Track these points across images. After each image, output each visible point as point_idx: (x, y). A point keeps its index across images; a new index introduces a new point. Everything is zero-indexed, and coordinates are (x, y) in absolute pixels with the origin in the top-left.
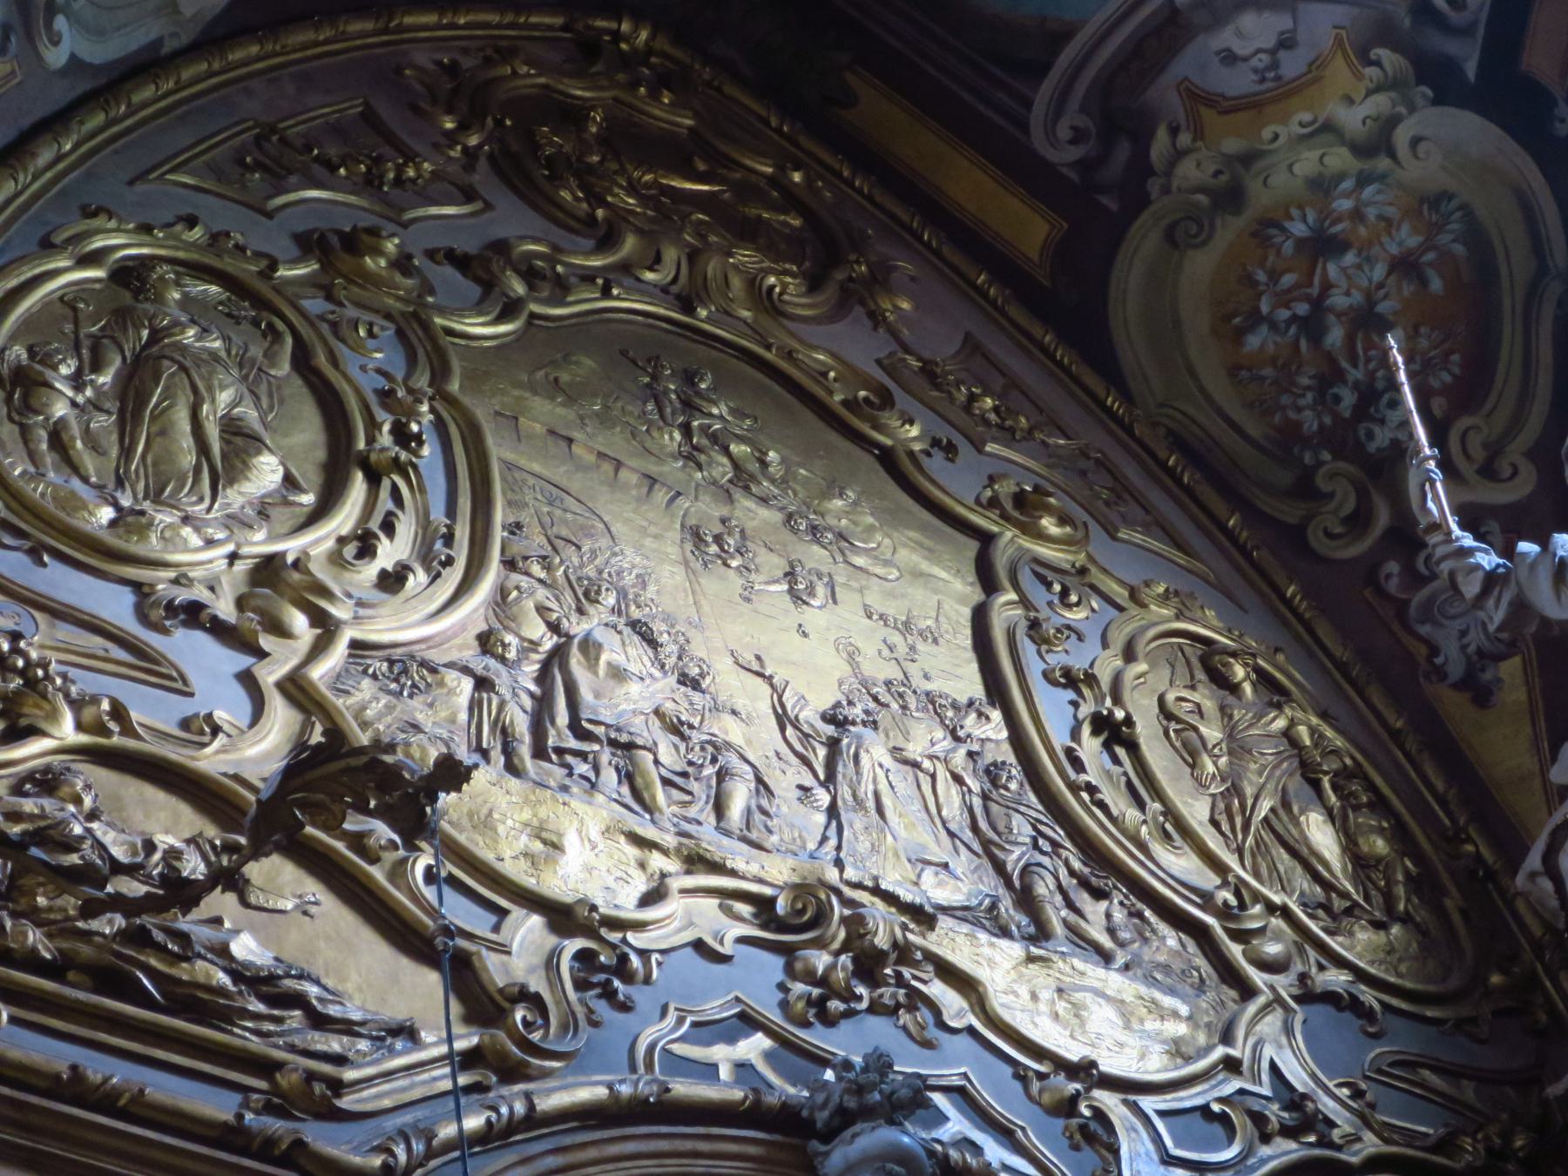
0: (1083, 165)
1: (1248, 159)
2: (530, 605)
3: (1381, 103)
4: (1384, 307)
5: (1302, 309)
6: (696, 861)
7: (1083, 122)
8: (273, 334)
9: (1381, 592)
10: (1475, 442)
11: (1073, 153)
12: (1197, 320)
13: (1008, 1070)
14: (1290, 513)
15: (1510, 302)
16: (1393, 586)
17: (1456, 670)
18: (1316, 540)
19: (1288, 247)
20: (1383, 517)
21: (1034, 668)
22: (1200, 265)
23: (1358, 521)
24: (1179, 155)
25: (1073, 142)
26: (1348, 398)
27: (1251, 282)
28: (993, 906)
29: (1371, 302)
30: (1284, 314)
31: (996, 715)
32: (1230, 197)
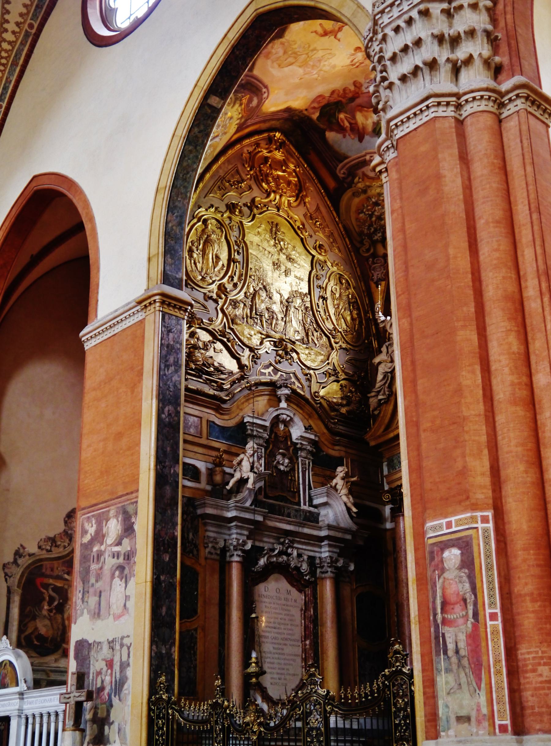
0: (343, 178)
1: (369, 187)
2: (251, 285)
5: (370, 213)
6: (268, 336)
7: (345, 171)
8: (222, 231)
11: (342, 176)
12: (353, 209)
13: (300, 368)
14: (358, 245)
16: (370, 263)
17: (375, 280)
18: (361, 251)
20: (372, 251)
21: (316, 284)
22: (356, 200)
23: (368, 250)
24: (359, 182)
25: (343, 174)
26: (372, 230)
27: (363, 206)
28: (303, 339)
30: (367, 213)
31: (309, 297)
32: (365, 191)
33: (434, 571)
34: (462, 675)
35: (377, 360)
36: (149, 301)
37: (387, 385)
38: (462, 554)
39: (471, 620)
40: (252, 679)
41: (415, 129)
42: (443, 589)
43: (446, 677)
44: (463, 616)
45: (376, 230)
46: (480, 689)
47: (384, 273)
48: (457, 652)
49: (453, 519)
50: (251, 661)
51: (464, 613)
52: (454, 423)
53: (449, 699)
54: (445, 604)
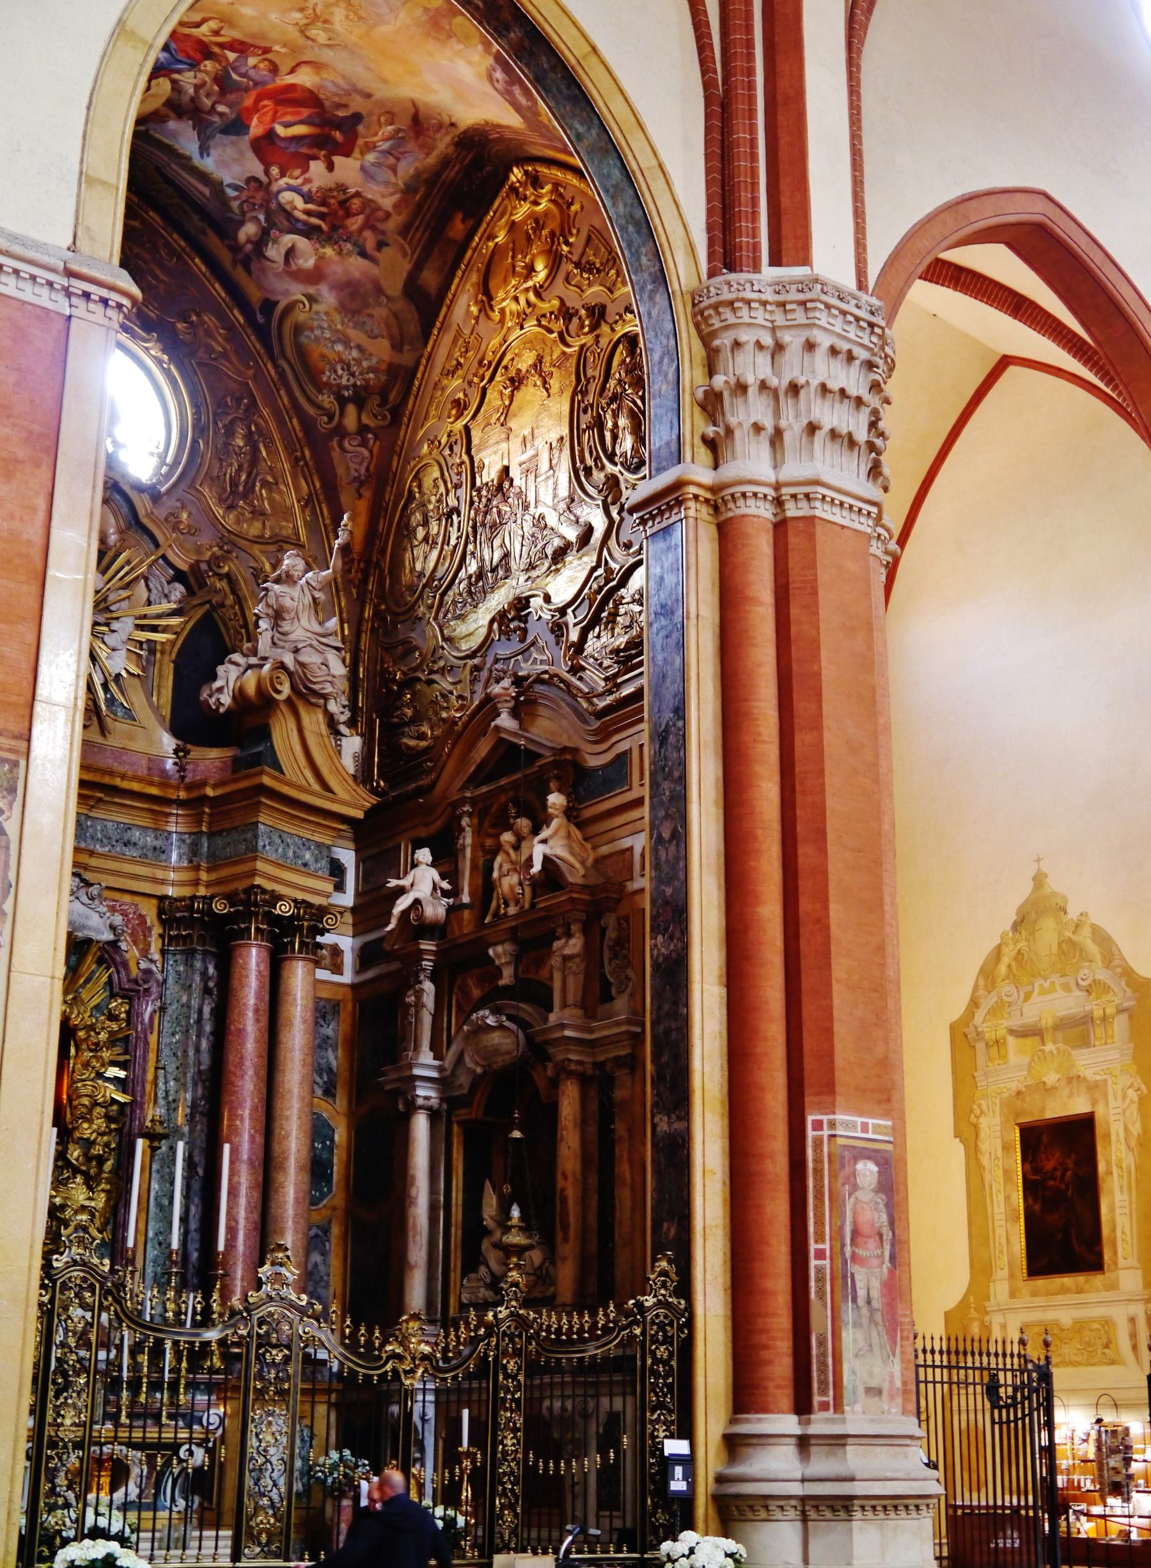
33: (844, 1184)
34: (874, 1333)
36: (105, 293)
38: (879, 1172)
39: (887, 1264)
41: (843, 527)
42: (855, 1214)
43: (854, 1333)
44: (878, 1257)
46: (894, 1355)
48: (869, 1302)
49: (871, 1121)
51: (879, 1252)
52: (876, 991)
53: (857, 1363)
54: (855, 1233)
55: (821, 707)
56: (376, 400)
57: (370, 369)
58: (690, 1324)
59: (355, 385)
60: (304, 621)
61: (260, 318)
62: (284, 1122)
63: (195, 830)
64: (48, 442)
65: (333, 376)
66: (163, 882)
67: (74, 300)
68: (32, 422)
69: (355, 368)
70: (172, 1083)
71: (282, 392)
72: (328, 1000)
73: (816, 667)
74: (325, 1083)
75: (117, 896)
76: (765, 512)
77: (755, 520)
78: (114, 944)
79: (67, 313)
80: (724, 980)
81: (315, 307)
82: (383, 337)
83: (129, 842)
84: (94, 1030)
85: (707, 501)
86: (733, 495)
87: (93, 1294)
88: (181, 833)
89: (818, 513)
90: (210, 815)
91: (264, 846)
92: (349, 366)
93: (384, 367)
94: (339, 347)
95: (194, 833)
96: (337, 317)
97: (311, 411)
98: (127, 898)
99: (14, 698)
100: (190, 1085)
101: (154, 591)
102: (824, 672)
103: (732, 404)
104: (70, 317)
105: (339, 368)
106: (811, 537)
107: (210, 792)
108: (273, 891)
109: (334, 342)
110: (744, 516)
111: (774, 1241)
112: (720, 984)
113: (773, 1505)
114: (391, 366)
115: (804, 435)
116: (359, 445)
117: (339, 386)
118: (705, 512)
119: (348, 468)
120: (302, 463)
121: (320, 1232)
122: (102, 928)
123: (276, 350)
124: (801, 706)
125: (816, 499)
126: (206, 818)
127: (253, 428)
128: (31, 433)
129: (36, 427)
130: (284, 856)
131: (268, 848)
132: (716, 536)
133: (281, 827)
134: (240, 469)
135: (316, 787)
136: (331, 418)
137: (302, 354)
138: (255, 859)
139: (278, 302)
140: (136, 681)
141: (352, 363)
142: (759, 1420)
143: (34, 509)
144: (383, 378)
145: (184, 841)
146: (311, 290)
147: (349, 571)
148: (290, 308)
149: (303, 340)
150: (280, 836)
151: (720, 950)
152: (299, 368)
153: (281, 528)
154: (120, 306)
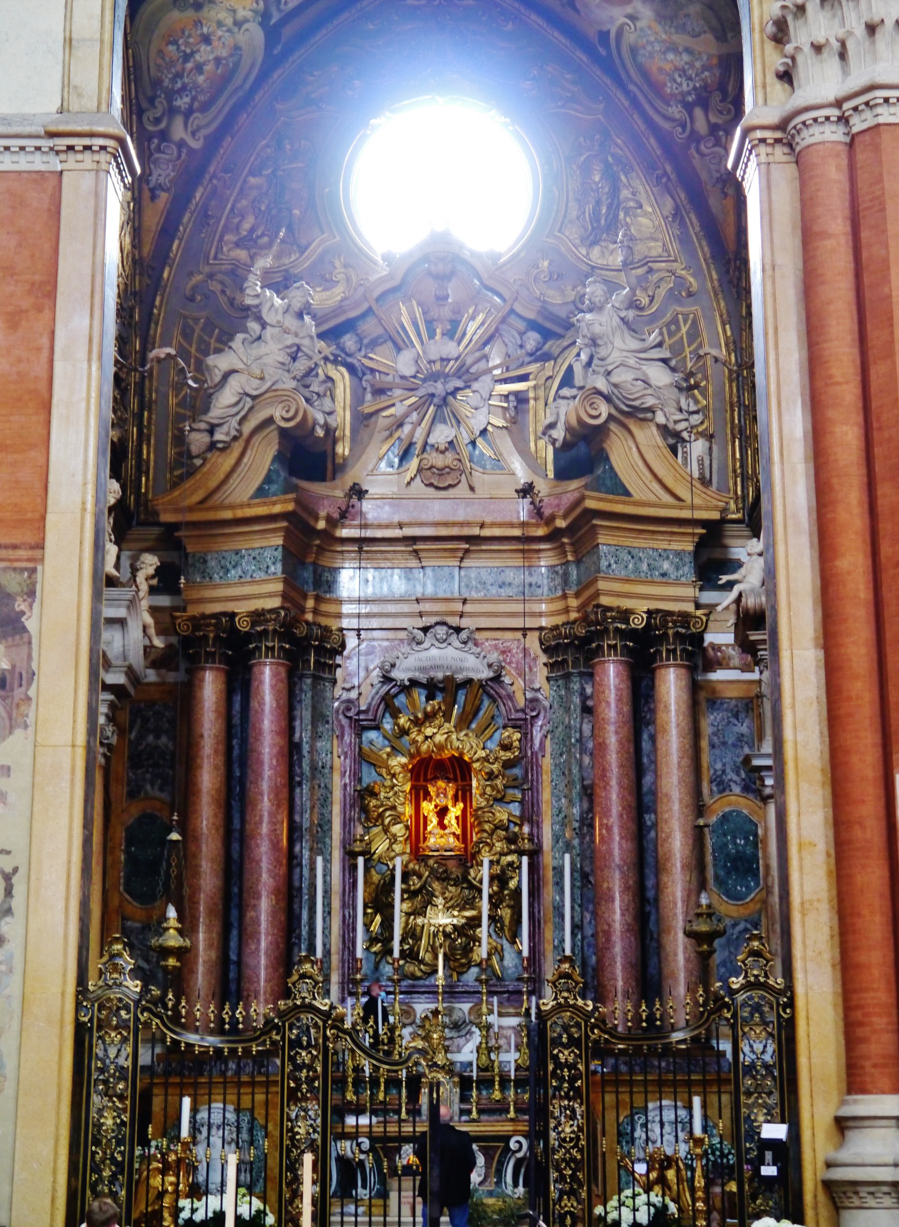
3: (249, 14)
4: (207, 68)
5: (188, 51)
9: (149, 145)
10: (197, 122)
14: (145, 105)
15: (230, 88)
16: (153, 146)
17: (152, 185)
18: (145, 119)
19: (199, 32)
20: (163, 125)
27: (183, 33)
29: (204, 64)
35: (220, 363)
36: (87, 141)
37: (238, 417)
40: (166, 960)
45: (184, 88)
47: (170, 178)
50: (165, 925)
55: (892, 333)
56: (716, 97)
57: (705, 68)
58: (791, 1004)
59: (695, 88)
60: (618, 343)
61: (603, 52)
62: (663, 825)
63: (564, 561)
64: (48, 288)
65: (675, 86)
66: (540, 615)
67: (63, 156)
68: (34, 274)
69: (690, 72)
70: (563, 800)
71: (636, 116)
72: (737, 699)
73: (886, 290)
74: (743, 780)
75: (498, 634)
76: (833, 134)
77: (821, 147)
78: (497, 678)
79: (59, 169)
80: (822, 641)
81: (639, 24)
82: (705, 32)
83: (504, 583)
84: (488, 761)
85: (778, 141)
86: (795, 127)
87: (129, 1012)
88: (554, 566)
89: (881, 120)
90: (572, 544)
91: (610, 565)
92: (684, 71)
93: (715, 61)
94: (671, 56)
95: (564, 564)
96: (658, 28)
97: (666, 125)
98: (509, 635)
99: (30, 515)
100: (577, 801)
101: (510, 345)
102: (894, 294)
103: (795, 28)
104: (61, 172)
105: (676, 76)
106: (876, 148)
107: (561, 523)
108: (618, 607)
109: (664, 53)
110: (809, 146)
111: (865, 912)
112: (816, 647)
113: (863, 1191)
114: (720, 57)
115: (867, 37)
116: (714, 146)
117: (683, 94)
118: (779, 152)
119: (710, 171)
120: (664, 180)
121: (749, 926)
122: (480, 667)
123: (624, 76)
124: (875, 335)
125: (876, 105)
126: (568, 548)
127: (610, 159)
128: (33, 284)
129: (37, 278)
130: (637, 570)
131: (614, 566)
132: (797, 174)
133: (629, 544)
134: (598, 203)
135: (667, 498)
136: (684, 126)
137: (645, 74)
138: (596, 580)
139: (608, 32)
140: (504, 431)
141: (686, 67)
142: (855, 1101)
143: (39, 349)
144: (717, 73)
145: (557, 573)
146: (629, 10)
147: (728, 272)
148: (620, 33)
149: (641, 59)
150: (629, 553)
151: (815, 611)
152: (645, 88)
153: (650, 249)
154: (103, 148)
